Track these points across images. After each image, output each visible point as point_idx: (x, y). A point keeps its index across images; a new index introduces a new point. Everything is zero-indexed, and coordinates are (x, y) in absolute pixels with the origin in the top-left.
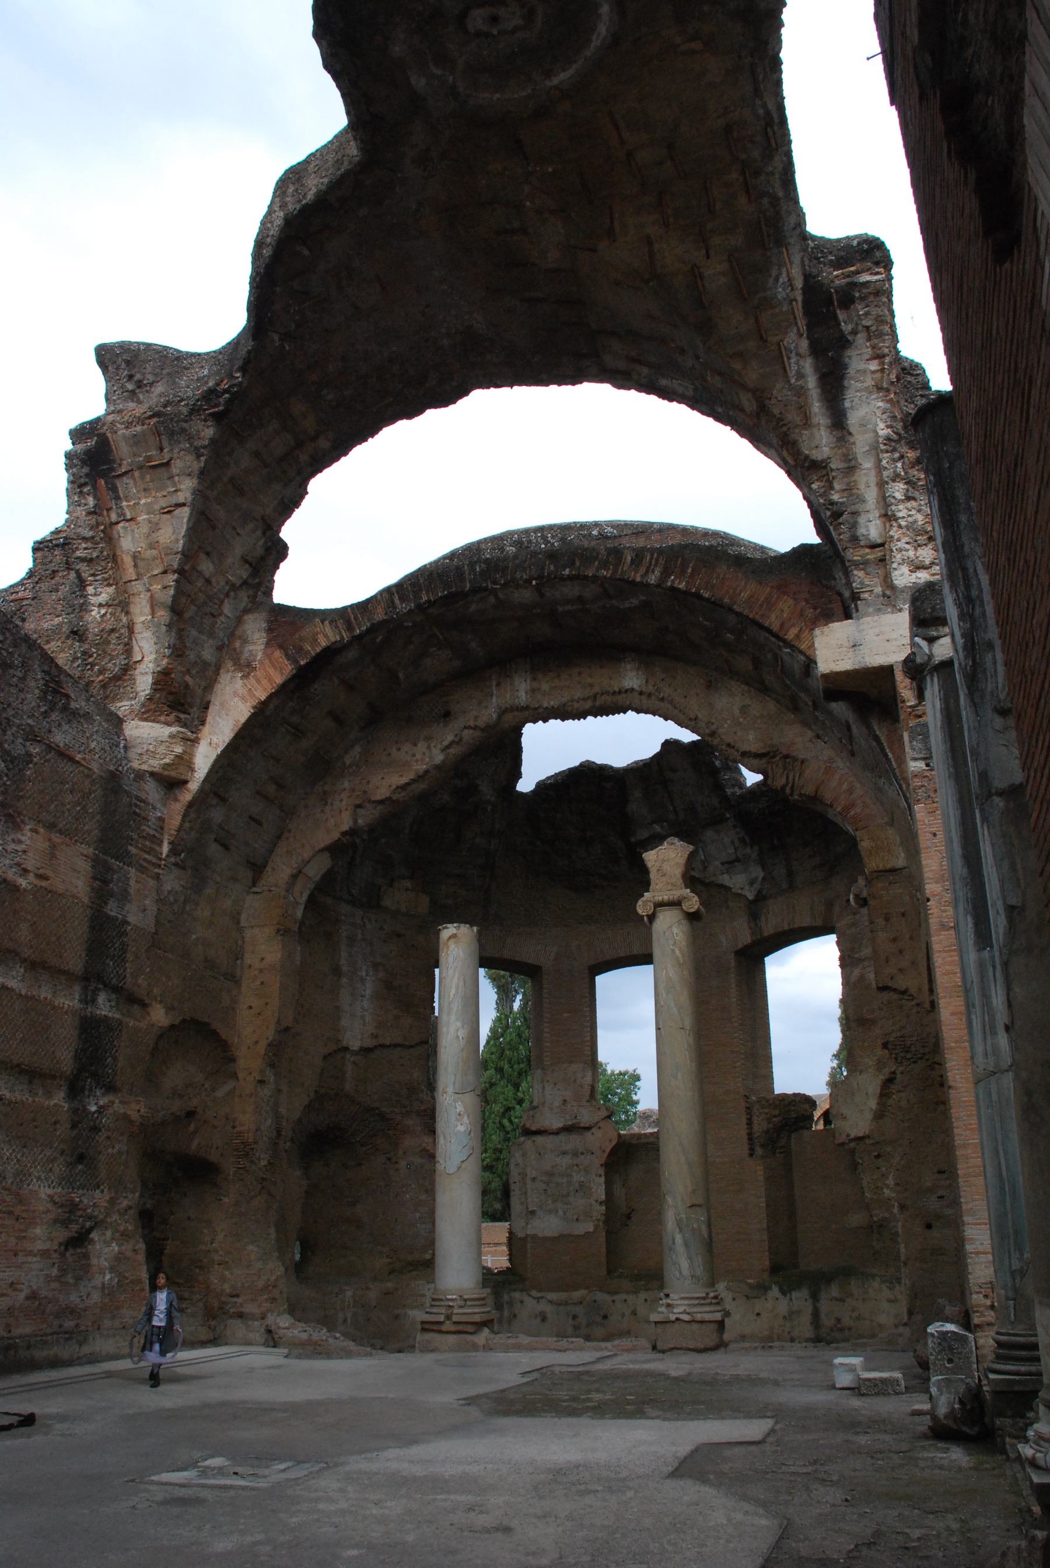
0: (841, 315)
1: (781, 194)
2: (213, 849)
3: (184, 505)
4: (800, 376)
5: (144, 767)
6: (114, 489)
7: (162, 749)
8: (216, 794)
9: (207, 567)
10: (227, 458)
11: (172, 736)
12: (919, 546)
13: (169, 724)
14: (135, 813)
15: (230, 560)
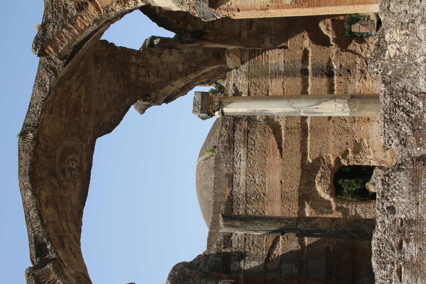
0: (69, 54)
1: (52, 91)
2: (254, 29)
3: (171, 85)
4: (88, 44)
5: (240, 61)
6: (172, 94)
7: (233, 58)
8: (240, 38)
9: (181, 67)
10: (155, 84)
11: (229, 57)
12: (129, 4)
13: (225, 58)
14: (254, 63)
15: (174, 60)
